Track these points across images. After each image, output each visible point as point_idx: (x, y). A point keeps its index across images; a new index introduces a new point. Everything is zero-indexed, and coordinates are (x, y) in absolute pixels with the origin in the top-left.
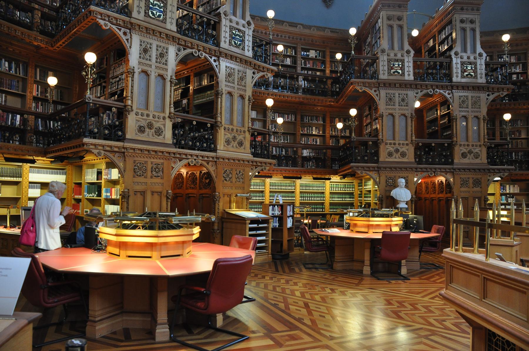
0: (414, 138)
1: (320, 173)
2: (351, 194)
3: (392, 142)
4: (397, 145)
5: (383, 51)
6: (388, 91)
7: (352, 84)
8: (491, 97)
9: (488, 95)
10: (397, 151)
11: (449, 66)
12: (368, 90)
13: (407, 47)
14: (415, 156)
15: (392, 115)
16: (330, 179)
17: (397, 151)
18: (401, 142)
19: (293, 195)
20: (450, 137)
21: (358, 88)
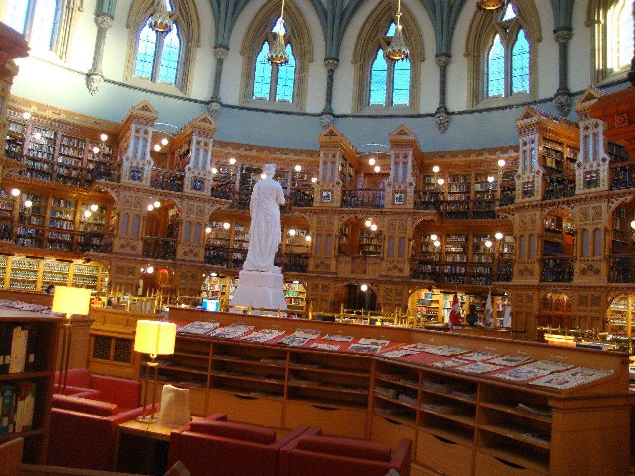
0: (144, 235)
1: (65, 256)
2: (96, 277)
3: (126, 236)
4: (129, 240)
5: (127, 159)
6: (127, 194)
7: (96, 184)
8: (214, 208)
9: (212, 206)
10: (128, 245)
11: (182, 178)
12: (109, 190)
13: (148, 157)
14: (143, 250)
15: (127, 214)
16: (72, 262)
17: (128, 245)
18: (133, 238)
19: (35, 274)
20: (176, 238)
21: (101, 188)
